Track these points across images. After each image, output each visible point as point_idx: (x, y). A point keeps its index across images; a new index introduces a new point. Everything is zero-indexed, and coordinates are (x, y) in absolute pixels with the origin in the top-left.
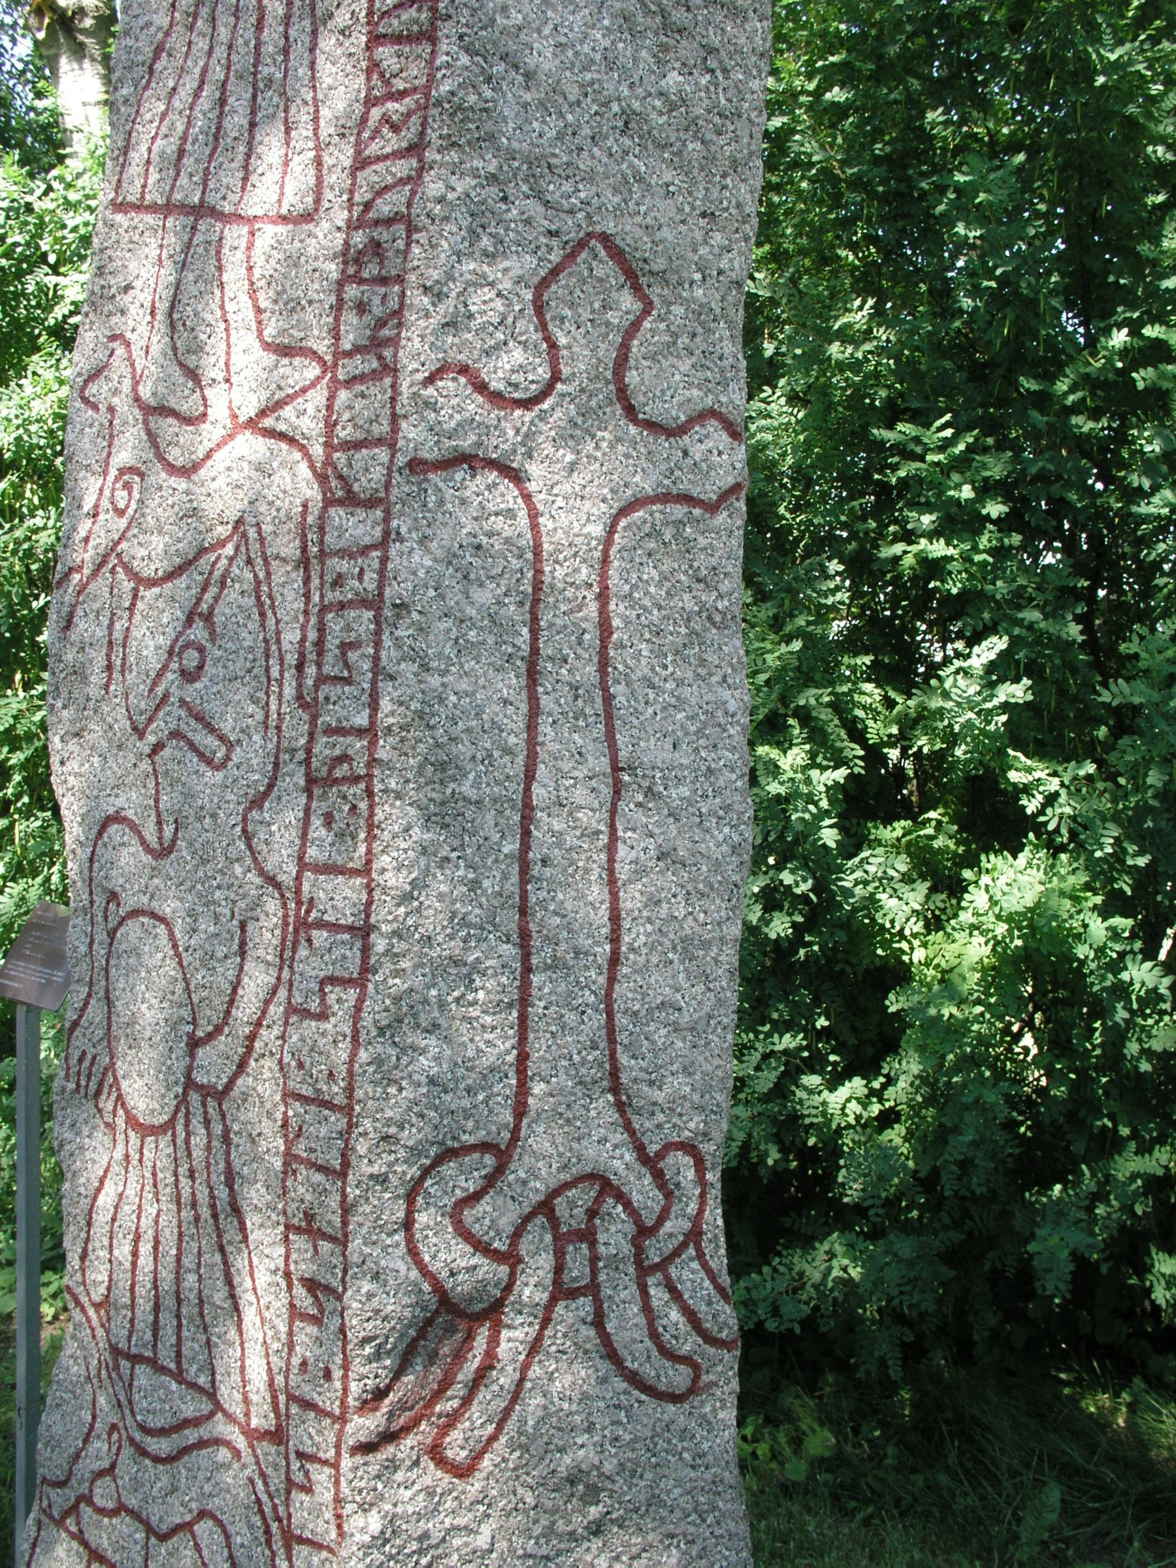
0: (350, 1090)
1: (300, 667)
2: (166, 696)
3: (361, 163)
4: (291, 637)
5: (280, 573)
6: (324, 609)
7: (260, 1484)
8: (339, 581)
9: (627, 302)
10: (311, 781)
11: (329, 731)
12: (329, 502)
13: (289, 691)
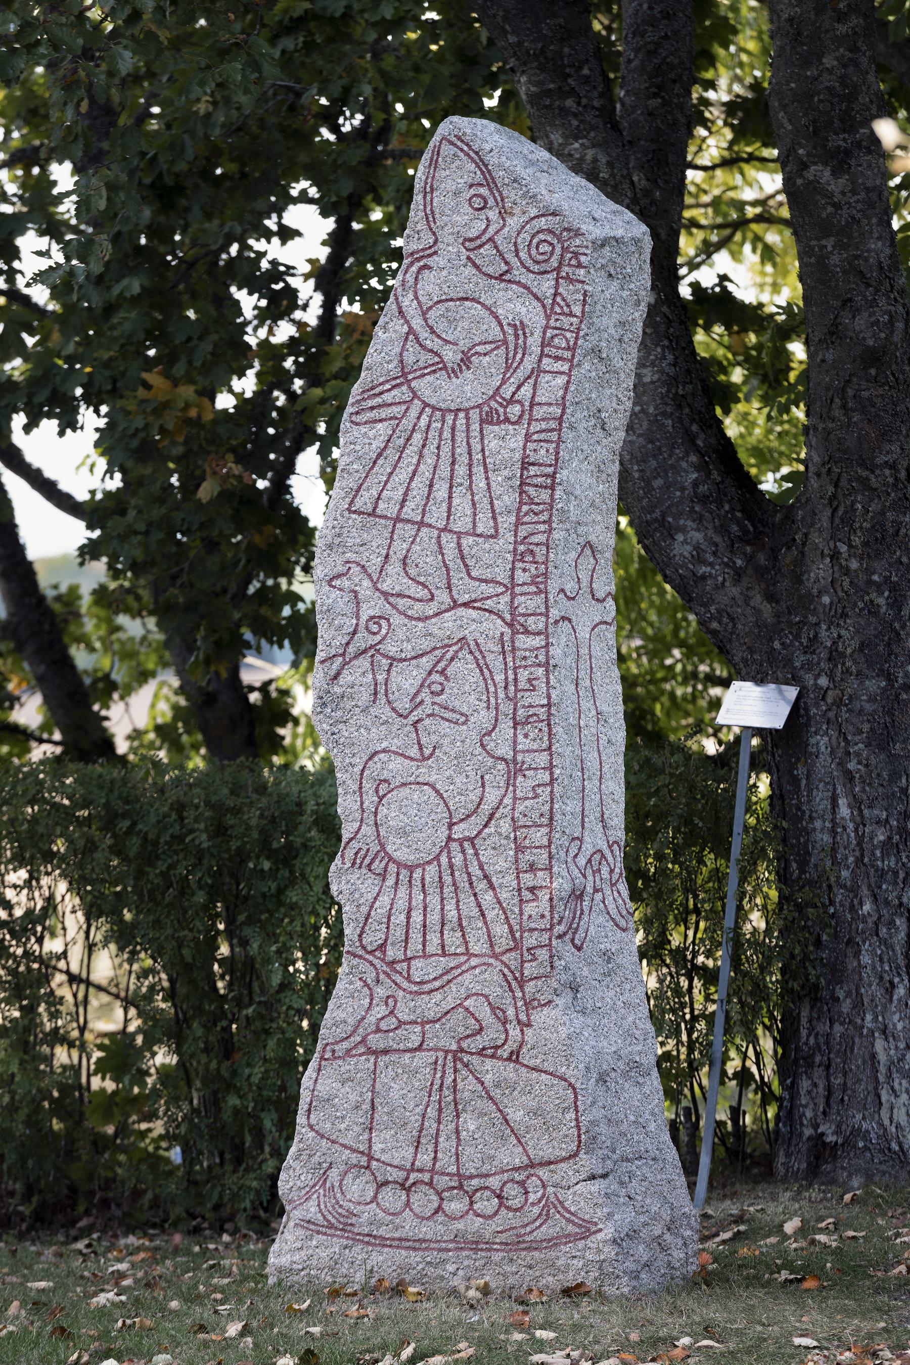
0: (551, 819)
1: (506, 688)
2: (422, 702)
3: (518, 523)
4: (499, 678)
5: (490, 658)
6: (515, 668)
7: (506, 971)
8: (525, 658)
9: (592, 561)
10: (516, 724)
11: (524, 707)
12: (513, 634)
13: (501, 695)
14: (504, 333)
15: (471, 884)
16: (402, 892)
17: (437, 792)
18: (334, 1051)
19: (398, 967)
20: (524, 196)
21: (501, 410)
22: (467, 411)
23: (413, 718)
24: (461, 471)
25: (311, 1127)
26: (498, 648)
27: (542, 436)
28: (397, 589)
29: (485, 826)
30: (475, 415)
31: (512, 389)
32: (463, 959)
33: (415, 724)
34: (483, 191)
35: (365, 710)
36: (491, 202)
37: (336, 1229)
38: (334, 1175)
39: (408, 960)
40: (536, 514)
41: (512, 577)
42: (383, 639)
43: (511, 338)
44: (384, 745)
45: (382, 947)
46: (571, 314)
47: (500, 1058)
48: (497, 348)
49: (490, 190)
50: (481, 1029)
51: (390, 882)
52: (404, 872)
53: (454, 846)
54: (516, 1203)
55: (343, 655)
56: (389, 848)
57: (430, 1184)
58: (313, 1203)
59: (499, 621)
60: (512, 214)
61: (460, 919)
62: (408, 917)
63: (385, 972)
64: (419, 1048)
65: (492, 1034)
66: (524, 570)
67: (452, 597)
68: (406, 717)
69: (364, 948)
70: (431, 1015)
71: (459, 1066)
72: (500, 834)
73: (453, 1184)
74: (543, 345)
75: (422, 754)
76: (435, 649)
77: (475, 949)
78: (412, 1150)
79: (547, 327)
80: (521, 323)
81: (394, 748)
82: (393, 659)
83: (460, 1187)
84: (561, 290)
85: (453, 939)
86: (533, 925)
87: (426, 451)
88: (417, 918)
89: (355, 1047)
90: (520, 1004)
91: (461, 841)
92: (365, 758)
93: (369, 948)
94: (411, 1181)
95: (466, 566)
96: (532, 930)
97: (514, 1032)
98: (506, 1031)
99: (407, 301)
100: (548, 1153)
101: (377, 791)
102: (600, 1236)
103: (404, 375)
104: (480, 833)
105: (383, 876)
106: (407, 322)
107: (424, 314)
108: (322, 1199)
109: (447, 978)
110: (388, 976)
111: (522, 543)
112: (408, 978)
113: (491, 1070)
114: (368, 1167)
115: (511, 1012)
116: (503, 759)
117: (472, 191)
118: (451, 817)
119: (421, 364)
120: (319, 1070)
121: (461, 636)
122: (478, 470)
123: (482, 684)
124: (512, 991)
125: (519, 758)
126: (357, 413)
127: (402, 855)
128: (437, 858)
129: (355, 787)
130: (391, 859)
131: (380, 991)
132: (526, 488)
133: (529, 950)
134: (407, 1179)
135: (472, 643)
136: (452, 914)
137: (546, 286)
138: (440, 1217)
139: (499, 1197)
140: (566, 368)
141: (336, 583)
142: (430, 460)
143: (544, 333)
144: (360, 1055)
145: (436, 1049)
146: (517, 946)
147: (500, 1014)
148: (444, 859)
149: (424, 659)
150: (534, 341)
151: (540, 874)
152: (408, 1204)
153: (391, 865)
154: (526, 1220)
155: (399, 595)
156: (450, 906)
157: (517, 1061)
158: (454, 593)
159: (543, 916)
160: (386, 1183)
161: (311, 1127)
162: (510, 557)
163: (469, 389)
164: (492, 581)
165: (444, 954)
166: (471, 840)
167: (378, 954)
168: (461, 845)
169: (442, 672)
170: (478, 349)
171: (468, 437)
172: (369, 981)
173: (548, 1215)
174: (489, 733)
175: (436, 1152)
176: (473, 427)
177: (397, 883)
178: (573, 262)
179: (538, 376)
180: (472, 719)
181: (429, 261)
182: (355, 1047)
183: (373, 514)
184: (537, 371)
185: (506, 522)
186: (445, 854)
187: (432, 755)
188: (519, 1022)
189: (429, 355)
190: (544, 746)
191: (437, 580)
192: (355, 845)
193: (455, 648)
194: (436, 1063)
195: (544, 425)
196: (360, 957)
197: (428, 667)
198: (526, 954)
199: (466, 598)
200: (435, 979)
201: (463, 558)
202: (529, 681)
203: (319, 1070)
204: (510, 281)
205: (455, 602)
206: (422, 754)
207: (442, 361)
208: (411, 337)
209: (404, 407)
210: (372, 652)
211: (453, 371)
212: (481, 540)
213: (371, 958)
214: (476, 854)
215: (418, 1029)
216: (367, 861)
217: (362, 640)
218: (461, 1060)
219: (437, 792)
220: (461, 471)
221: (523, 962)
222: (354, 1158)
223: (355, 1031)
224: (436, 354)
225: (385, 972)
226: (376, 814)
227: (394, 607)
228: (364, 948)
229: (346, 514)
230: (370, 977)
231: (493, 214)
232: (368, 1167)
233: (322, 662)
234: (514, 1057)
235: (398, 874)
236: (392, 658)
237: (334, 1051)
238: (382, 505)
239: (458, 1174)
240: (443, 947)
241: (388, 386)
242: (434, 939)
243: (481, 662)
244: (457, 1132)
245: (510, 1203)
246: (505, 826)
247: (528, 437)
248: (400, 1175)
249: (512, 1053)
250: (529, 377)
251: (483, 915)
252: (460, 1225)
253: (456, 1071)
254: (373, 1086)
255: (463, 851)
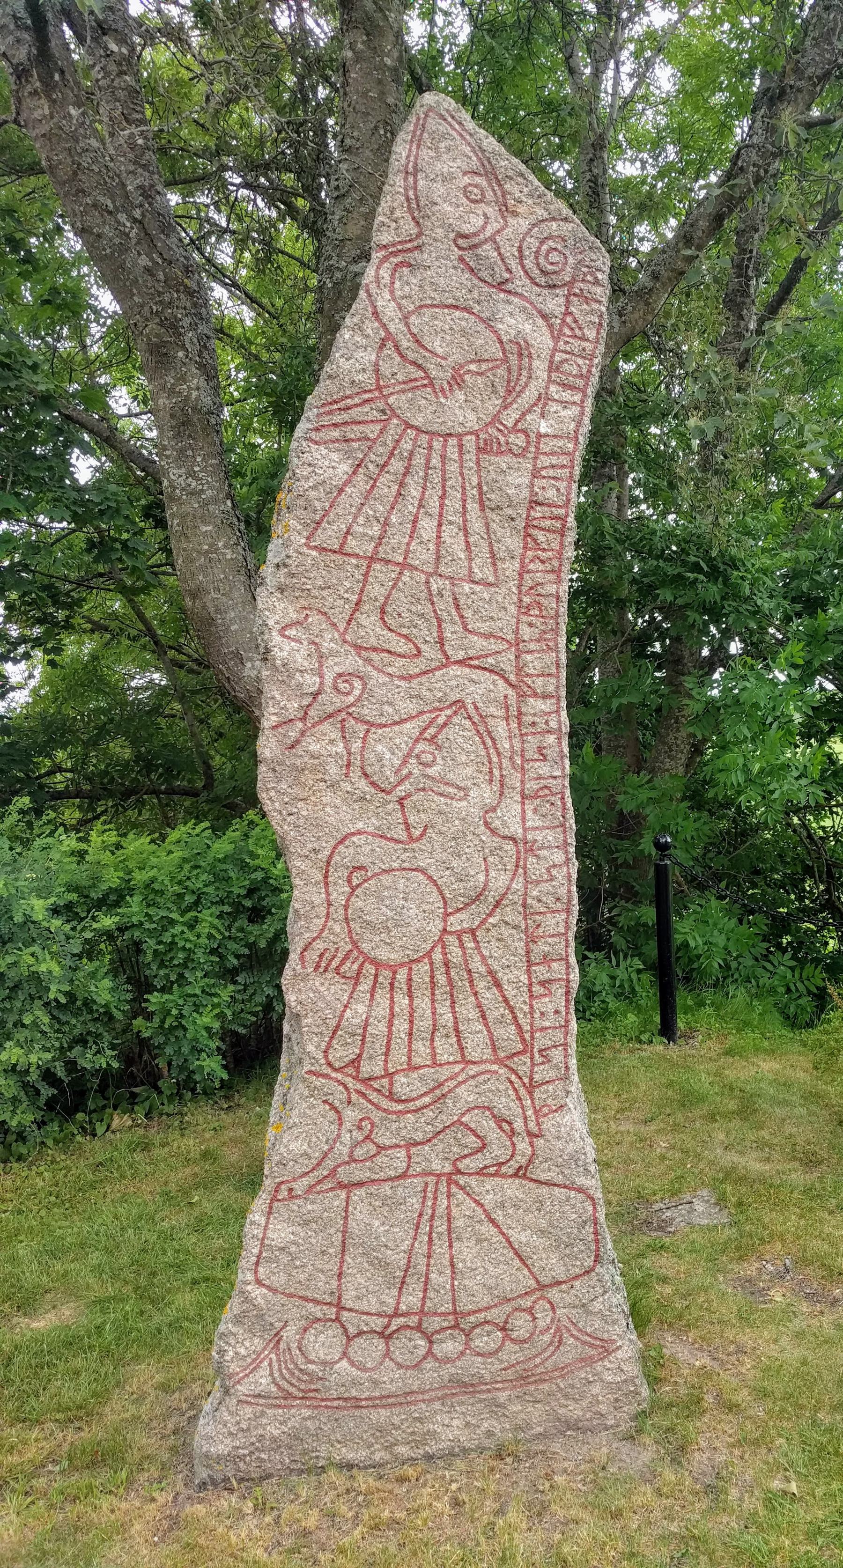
2: (410, 773)
3: (523, 572)
14: (504, 351)
15: (471, 982)
16: (382, 998)
17: (430, 878)
18: (291, 1190)
19: (376, 1085)
20: (530, 195)
21: (502, 439)
22: (460, 437)
23: (401, 791)
24: (453, 503)
25: (259, 1282)
26: (502, 713)
27: (551, 472)
28: (373, 642)
29: (490, 915)
30: (470, 442)
31: (516, 416)
32: (458, 1068)
33: (401, 801)
34: (478, 180)
35: (333, 786)
36: (489, 195)
37: (295, 1398)
38: (290, 1334)
39: (390, 1075)
40: (543, 562)
41: (517, 632)
42: (359, 699)
43: (513, 359)
44: (360, 825)
45: (355, 1062)
46: (583, 338)
47: (504, 1176)
48: (497, 367)
49: (489, 181)
50: (484, 1146)
51: (365, 986)
52: (385, 976)
53: (451, 939)
54: (522, 1334)
55: (303, 719)
56: (365, 947)
57: (419, 1328)
58: (264, 1371)
59: (501, 682)
60: (515, 214)
61: (456, 1023)
62: (390, 1024)
63: (358, 1092)
64: (404, 1175)
65: (498, 1149)
66: (531, 625)
67: (445, 653)
68: (389, 793)
69: (330, 1064)
70: (419, 1136)
71: (454, 1189)
72: (507, 923)
73: (445, 1324)
74: (550, 370)
75: (410, 836)
76: (421, 713)
77: (473, 1054)
78: (395, 1292)
79: (555, 350)
80: (526, 342)
81: (371, 829)
82: (372, 724)
83: (456, 1326)
84: (573, 309)
85: (446, 1049)
86: (547, 1024)
87: (408, 480)
88: (401, 1026)
89: (319, 1182)
90: (530, 1113)
91: (459, 935)
92: (333, 843)
93: (337, 1065)
94: (393, 1327)
95: (462, 617)
96: (543, 1029)
97: (523, 1146)
98: (513, 1144)
99: (383, 301)
100: (560, 1273)
101: (349, 881)
102: (619, 1354)
103: (379, 388)
104: (483, 922)
105: (357, 979)
106: (384, 326)
107: (405, 318)
108: (275, 1365)
109: (439, 1095)
110: (364, 1095)
111: (527, 594)
112: (391, 1096)
113: (490, 1191)
114: (337, 1319)
115: (519, 1125)
116: (513, 839)
117: (467, 180)
118: (445, 908)
119: (400, 377)
120: (270, 1213)
121: (458, 697)
122: (473, 507)
123: (483, 753)
124: (520, 1099)
125: (529, 837)
126: (317, 430)
127: (383, 954)
128: (429, 954)
129: (320, 877)
130: (367, 958)
131: (351, 1115)
132: (535, 532)
133: (540, 1051)
134: (386, 1327)
135: (470, 707)
136: (447, 1018)
137: (554, 304)
138: (429, 1364)
139: (503, 1329)
140: (577, 398)
141: (292, 632)
142: (414, 492)
143: (552, 356)
144: (327, 1191)
145: (426, 1174)
146: (527, 1048)
147: (506, 1126)
148: (437, 956)
149: (408, 725)
150: (540, 367)
151: (555, 965)
152: (387, 1354)
153: (367, 964)
154: (534, 1351)
155: (375, 649)
156: (444, 1010)
157: (524, 1176)
158: (446, 648)
159: (557, 1012)
160: (360, 1333)
161: (259, 1282)
162: (513, 610)
163: (462, 412)
164: (492, 635)
165: (435, 1064)
166: (473, 932)
167: (350, 1070)
168: (460, 939)
169: (432, 740)
170: (473, 367)
171: (461, 467)
172: (337, 1104)
173: (560, 1342)
174: (494, 809)
175: (425, 1291)
176: (466, 457)
177: (374, 986)
178: (589, 278)
179: (545, 404)
180: (471, 793)
181: (410, 257)
182: (319, 1182)
183: (340, 552)
184: (544, 399)
185: (511, 568)
186: (438, 949)
187: (422, 835)
188: (530, 1134)
189: (411, 368)
190: (556, 823)
191: (426, 632)
192: (319, 945)
193: (449, 712)
194: (425, 1191)
195: (554, 460)
196: (326, 1076)
197: (417, 732)
198: (537, 1055)
199: (461, 655)
200: (425, 1094)
201: (457, 607)
202: (540, 749)
203: (270, 1213)
204: (510, 292)
205: (448, 658)
206: (410, 836)
207: (428, 377)
208: (390, 344)
209: (378, 427)
210: (343, 715)
211: (442, 390)
212: (478, 588)
213: (339, 1076)
214: (478, 948)
215: (402, 1154)
216: (334, 964)
217: (331, 701)
218: (457, 1183)
219: (430, 878)
220: (453, 503)
221: (533, 1065)
222: (317, 1311)
223: (319, 1164)
224: (419, 367)
225: (358, 1092)
226: (346, 907)
227: (368, 661)
228: (330, 1064)
229: (305, 549)
230: (340, 1095)
231: (491, 211)
232: (337, 1319)
233: (274, 728)
234: (520, 1173)
235: (376, 976)
236: (367, 722)
237: (291, 1190)
238: (351, 542)
239: (455, 1312)
240: (434, 1055)
241: (357, 400)
242: (421, 1048)
243: (482, 729)
244: (452, 1265)
245: (514, 1335)
246: (512, 915)
247: (535, 474)
248: (378, 1323)
249: (520, 1168)
250: (536, 404)
251: (484, 1017)
252: (451, 1369)
253: (449, 1196)
254: (345, 1224)
255: (462, 945)
